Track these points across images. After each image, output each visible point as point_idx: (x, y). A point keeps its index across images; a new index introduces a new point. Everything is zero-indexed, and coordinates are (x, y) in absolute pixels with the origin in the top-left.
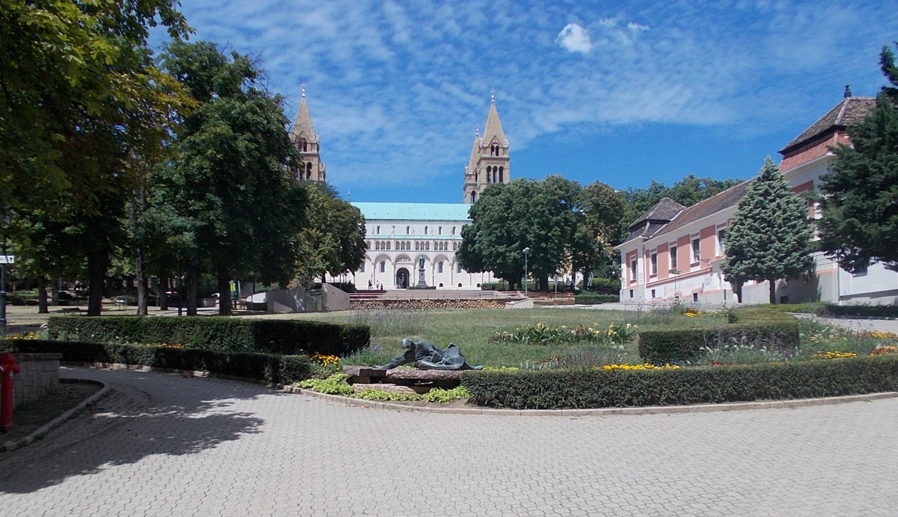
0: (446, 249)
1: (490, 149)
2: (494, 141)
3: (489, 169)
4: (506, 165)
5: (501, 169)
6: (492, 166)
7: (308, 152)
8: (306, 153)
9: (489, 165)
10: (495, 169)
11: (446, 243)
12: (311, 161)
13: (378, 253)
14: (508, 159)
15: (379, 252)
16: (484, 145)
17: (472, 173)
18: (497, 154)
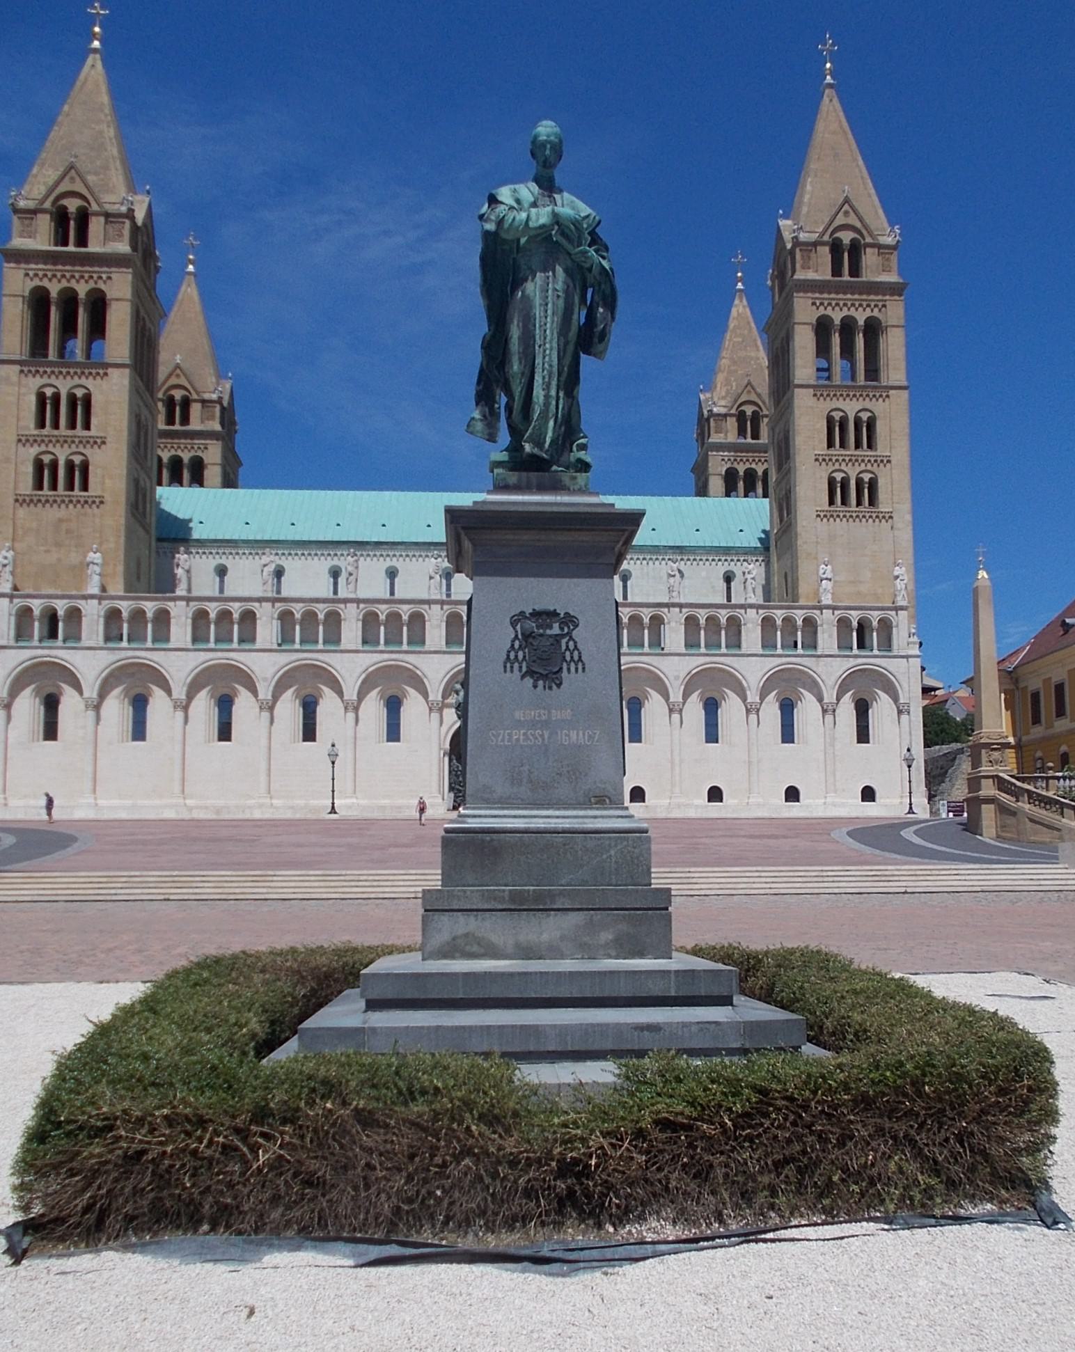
0: (656, 642)
1: (827, 249)
2: (841, 220)
3: (822, 328)
4: (894, 312)
5: (873, 330)
6: (837, 316)
7: (94, 247)
8: (83, 250)
9: (822, 311)
10: (848, 327)
11: (657, 621)
12: (102, 286)
13: (370, 660)
14: (895, 290)
15: (377, 657)
16: (803, 236)
17: (723, 411)
18: (855, 271)
